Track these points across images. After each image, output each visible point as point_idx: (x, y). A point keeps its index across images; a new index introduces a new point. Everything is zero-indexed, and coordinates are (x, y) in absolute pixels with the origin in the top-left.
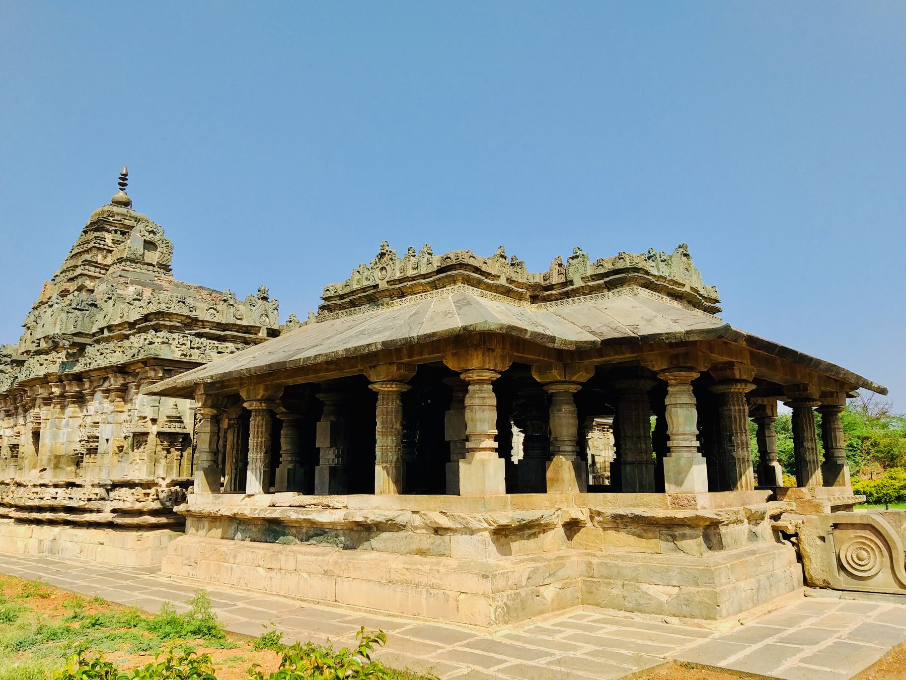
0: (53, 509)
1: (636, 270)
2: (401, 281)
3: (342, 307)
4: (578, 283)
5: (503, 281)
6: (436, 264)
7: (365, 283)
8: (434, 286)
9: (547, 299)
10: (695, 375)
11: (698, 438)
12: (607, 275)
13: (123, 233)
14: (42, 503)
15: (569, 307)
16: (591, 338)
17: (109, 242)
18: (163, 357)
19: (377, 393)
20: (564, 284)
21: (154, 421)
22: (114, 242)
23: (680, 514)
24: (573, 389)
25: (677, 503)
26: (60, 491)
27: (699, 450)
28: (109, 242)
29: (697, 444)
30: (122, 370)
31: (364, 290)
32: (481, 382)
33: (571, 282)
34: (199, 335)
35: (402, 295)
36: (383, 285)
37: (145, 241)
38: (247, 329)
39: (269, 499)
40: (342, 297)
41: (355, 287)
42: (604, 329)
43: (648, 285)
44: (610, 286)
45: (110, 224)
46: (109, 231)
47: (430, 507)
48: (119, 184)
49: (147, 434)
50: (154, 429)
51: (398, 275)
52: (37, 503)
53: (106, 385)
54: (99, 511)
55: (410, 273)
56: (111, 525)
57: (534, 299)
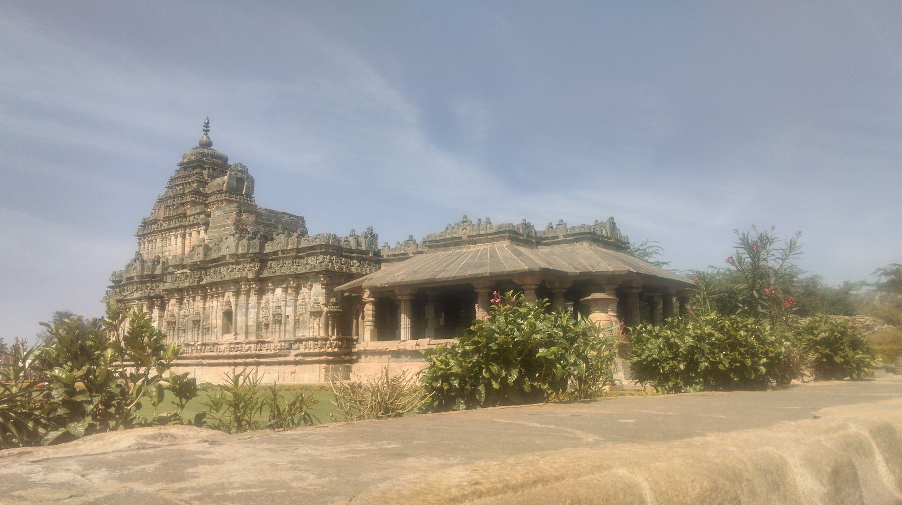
0: (247, 357)
4: (561, 238)
6: (495, 230)
7: (454, 235)
8: (493, 240)
12: (575, 235)
14: (238, 353)
15: (557, 249)
16: (574, 270)
19: (477, 294)
20: (554, 238)
22: (209, 176)
24: (564, 291)
26: (253, 346)
30: (297, 277)
31: (452, 239)
33: (558, 237)
35: (475, 243)
36: (464, 238)
40: (438, 241)
41: (448, 237)
42: (579, 267)
50: (325, 309)
52: (215, 354)
54: (285, 356)
55: (482, 232)
56: (296, 363)
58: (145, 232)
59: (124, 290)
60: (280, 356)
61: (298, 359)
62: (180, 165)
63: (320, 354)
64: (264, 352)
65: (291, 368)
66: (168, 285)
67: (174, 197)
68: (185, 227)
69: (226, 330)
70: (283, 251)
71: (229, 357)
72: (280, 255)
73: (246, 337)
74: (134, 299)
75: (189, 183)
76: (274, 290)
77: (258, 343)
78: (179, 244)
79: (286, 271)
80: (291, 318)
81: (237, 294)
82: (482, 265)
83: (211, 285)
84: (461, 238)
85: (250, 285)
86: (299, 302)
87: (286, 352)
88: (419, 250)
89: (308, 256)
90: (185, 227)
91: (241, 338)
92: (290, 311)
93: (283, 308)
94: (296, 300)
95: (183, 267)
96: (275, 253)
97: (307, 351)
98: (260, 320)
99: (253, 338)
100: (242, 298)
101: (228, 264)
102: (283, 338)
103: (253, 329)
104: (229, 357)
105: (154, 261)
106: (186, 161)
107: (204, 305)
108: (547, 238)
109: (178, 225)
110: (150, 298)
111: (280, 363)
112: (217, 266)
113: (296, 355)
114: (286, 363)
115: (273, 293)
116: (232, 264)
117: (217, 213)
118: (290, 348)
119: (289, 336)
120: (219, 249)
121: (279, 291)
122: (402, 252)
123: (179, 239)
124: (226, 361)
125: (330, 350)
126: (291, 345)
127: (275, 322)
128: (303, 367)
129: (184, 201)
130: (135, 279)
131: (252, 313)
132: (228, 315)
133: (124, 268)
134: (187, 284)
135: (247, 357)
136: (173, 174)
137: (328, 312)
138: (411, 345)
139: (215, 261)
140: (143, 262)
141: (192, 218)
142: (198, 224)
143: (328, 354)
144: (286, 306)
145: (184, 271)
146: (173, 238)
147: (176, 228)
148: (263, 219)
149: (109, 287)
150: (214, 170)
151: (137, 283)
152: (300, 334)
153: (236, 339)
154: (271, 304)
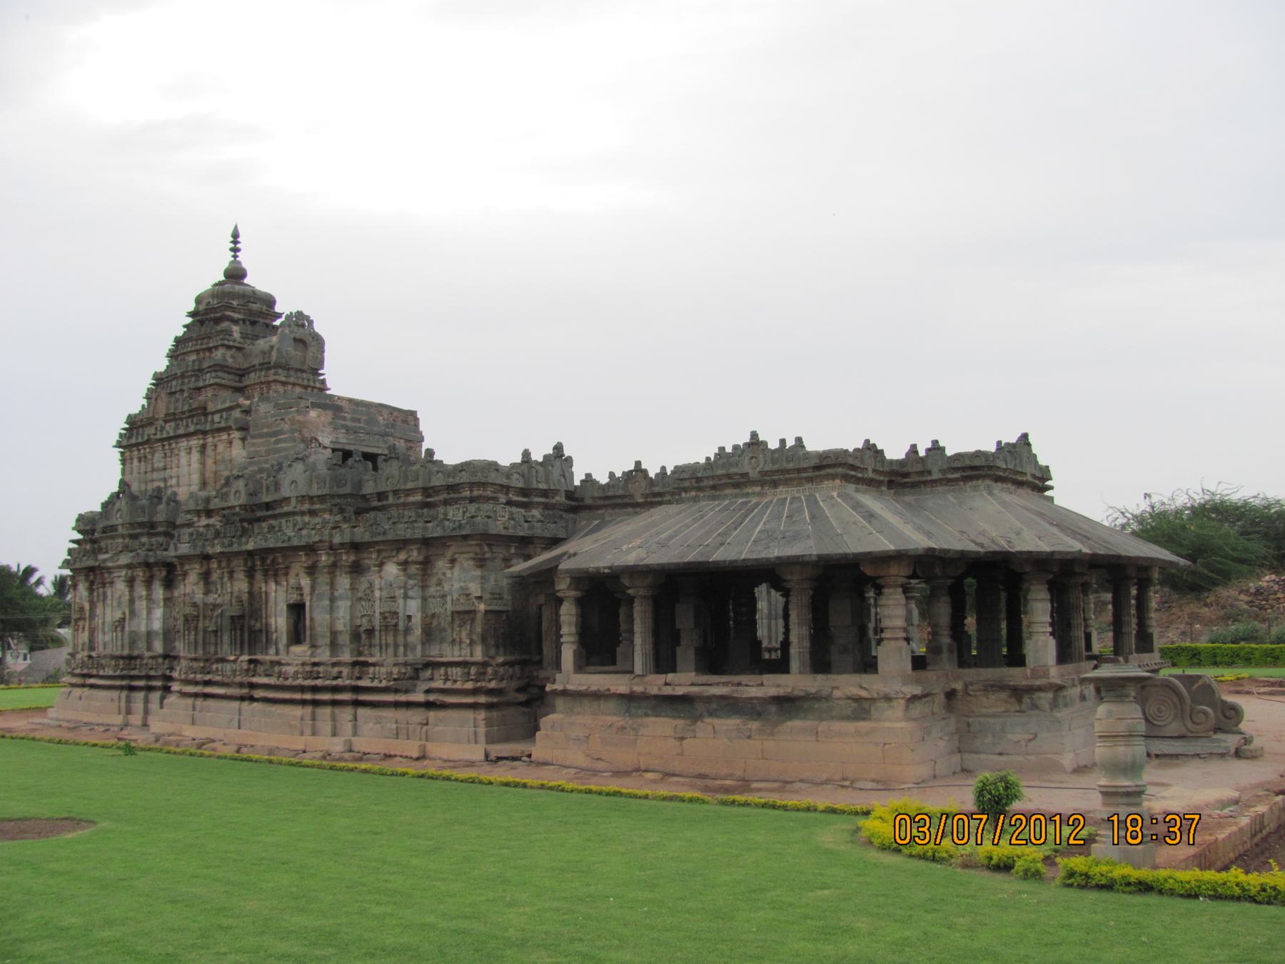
0: (335, 689)
1: (990, 468)
2: (773, 472)
3: (700, 489)
4: (936, 476)
5: (871, 475)
7: (733, 470)
8: (810, 480)
9: (904, 485)
10: (1051, 576)
11: (1052, 625)
12: (963, 469)
16: (972, 547)
17: (237, 335)
18: (492, 532)
20: (921, 473)
21: (480, 598)
22: (244, 336)
23: (1038, 683)
25: (1035, 673)
27: (1051, 634)
28: (237, 335)
29: (1050, 629)
30: (426, 542)
31: (728, 476)
32: (896, 586)
33: (930, 473)
34: (509, 503)
35: (775, 484)
36: (754, 474)
39: (661, 678)
40: (699, 480)
42: (980, 539)
43: (998, 479)
44: (966, 479)
45: (233, 309)
48: (232, 250)
49: (473, 612)
50: (482, 607)
51: (769, 467)
52: (272, 681)
53: (402, 556)
54: (407, 691)
56: (429, 705)
57: (890, 484)
58: (133, 441)
59: (100, 550)
60: (396, 691)
61: (432, 698)
62: (192, 314)
63: (475, 692)
64: (364, 683)
65: (416, 716)
66: (184, 549)
67: (183, 376)
68: (205, 433)
69: (297, 636)
70: (395, 492)
71: (302, 689)
72: (391, 500)
73: (333, 653)
74: (120, 567)
75: (210, 349)
76: (381, 565)
77: (355, 664)
78: (196, 466)
79: (403, 531)
80: (417, 620)
81: (312, 570)
82: (796, 537)
83: (263, 553)
84: (747, 474)
85: (336, 555)
86: (432, 590)
87: (409, 684)
88: (656, 489)
89: (446, 503)
90: (205, 433)
91: (324, 655)
92: (413, 607)
93: (401, 601)
94: (424, 587)
95: (209, 513)
96: (381, 496)
97: (449, 685)
98: (358, 622)
99: (346, 657)
100: (323, 579)
101: (294, 513)
102: (401, 659)
103: (344, 639)
104: (302, 689)
105: (151, 497)
106: (202, 307)
107: (251, 584)
108: (906, 475)
109: (192, 429)
110: (148, 565)
111: (397, 705)
112: (275, 517)
113: (428, 691)
114: (409, 705)
115: (380, 571)
116: (303, 513)
117: (264, 408)
118: (415, 677)
119: (416, 655)
120: (277, 486)
121: (391, 569)
122: (621, 492)
123: (196, 456)
124: (298, 696)
125: (493, 685)
126: (417, 670)
127: (386, 628)
128: (441, 714)
129: (201, 384)
130: (120, 530)
131: (343, 607)
132: (297, 610)
133: (98, 509)
134: (218, 549)
135: (335, 689)
136: (180, 332)
137: (486, 612)
138: (656, 684)
139: (268, 506)
140: (133, 498)
141: (217, 418)
142: (227, 429)
143: (490, 692)
144: (406, 597)
145: (212, 521)
146: (183, 454)
147: (188, 435)
148: (344, 419)
149: (73, 541)
150: (253, 323)
151: (123, 536)
152: (435, 652)
153: (312, 655)
154: (377, 594)
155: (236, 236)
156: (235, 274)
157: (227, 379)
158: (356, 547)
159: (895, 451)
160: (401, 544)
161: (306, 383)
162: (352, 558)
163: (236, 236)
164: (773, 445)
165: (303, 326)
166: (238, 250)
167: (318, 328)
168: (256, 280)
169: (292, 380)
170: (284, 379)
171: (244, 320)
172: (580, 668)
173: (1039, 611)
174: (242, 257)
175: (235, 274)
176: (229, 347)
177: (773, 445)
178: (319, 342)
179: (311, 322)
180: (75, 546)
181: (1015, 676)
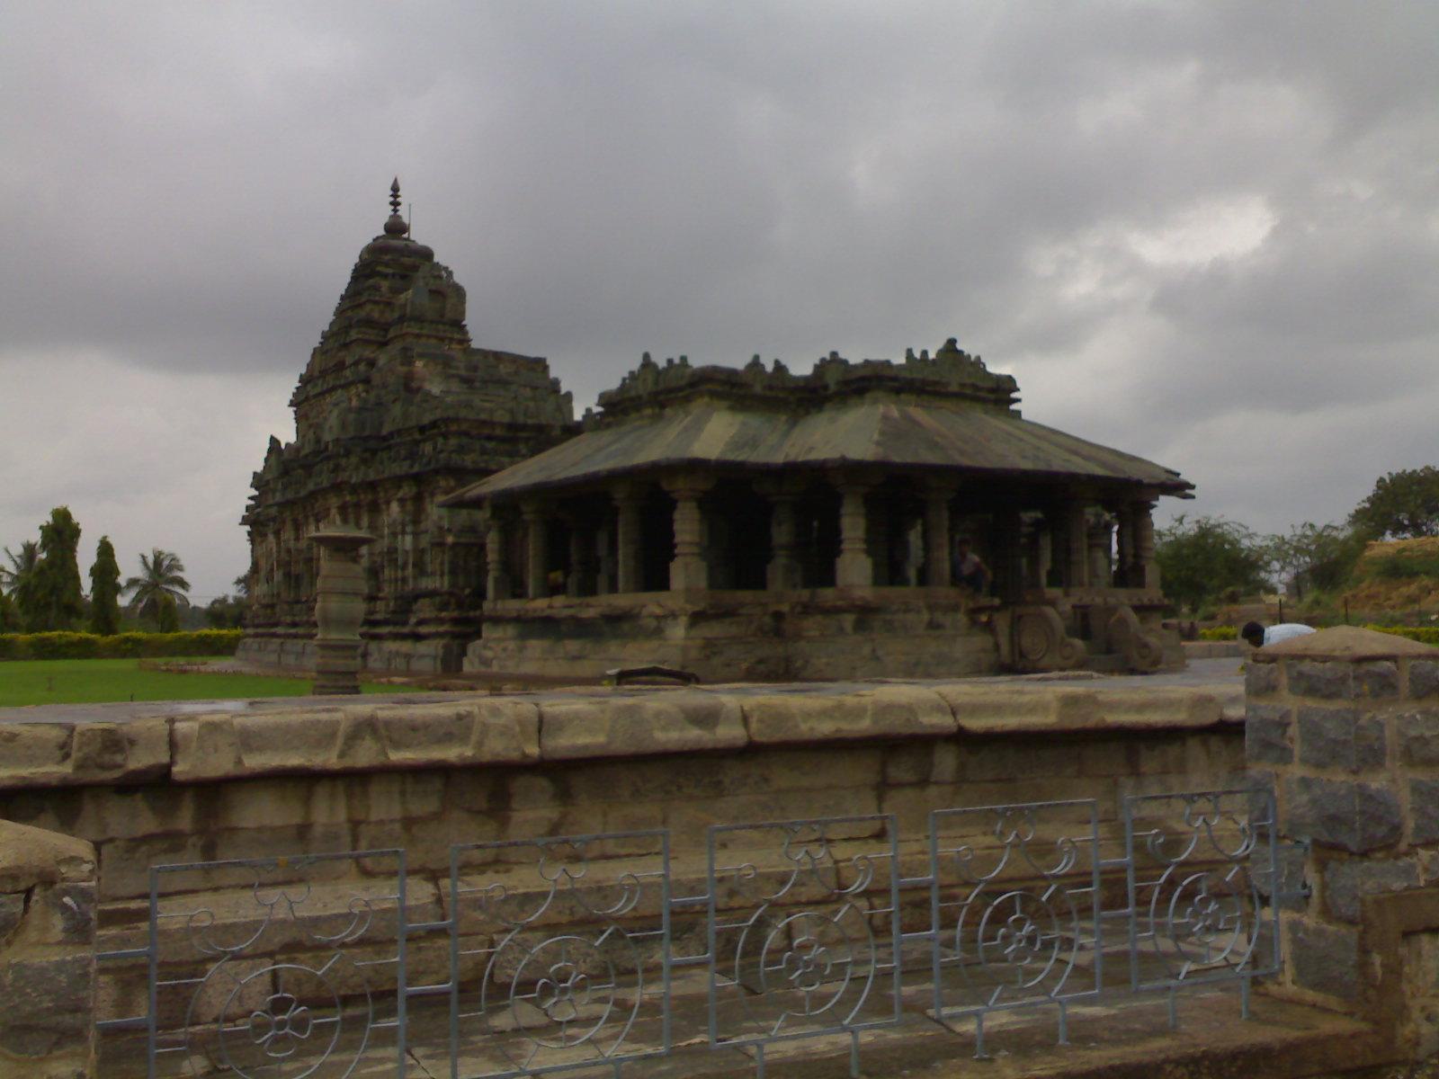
13: (403, 277)
37: (430, 291)
38: (540, 428)
46: (385, 276)
47: (651, 603)
48: (391, 203)
148: (457, 368)
155: (395, 189)
156: (396, 228)
157: (372, 334)
158: (372, 486)
159: (801, 367)
160: (398, 481)
161: (441, 334)
162: (370, 497)
163: (395, 189)
164: (662, 364)
165: (440, 277)
166: (399, 204)
167: (457, 278)
168: (419, 235)
169: (425, 332)
170: (417, 331)
171: (393, 275)
172: (499, 595)
173: (853, 526)
174: (402, 211)
175: (396, 228)
176: (376, 303)
177: (662, 364)
178: (460, 293)
179: (450, 274)
180: (252, 502)
181: (827, 595)
